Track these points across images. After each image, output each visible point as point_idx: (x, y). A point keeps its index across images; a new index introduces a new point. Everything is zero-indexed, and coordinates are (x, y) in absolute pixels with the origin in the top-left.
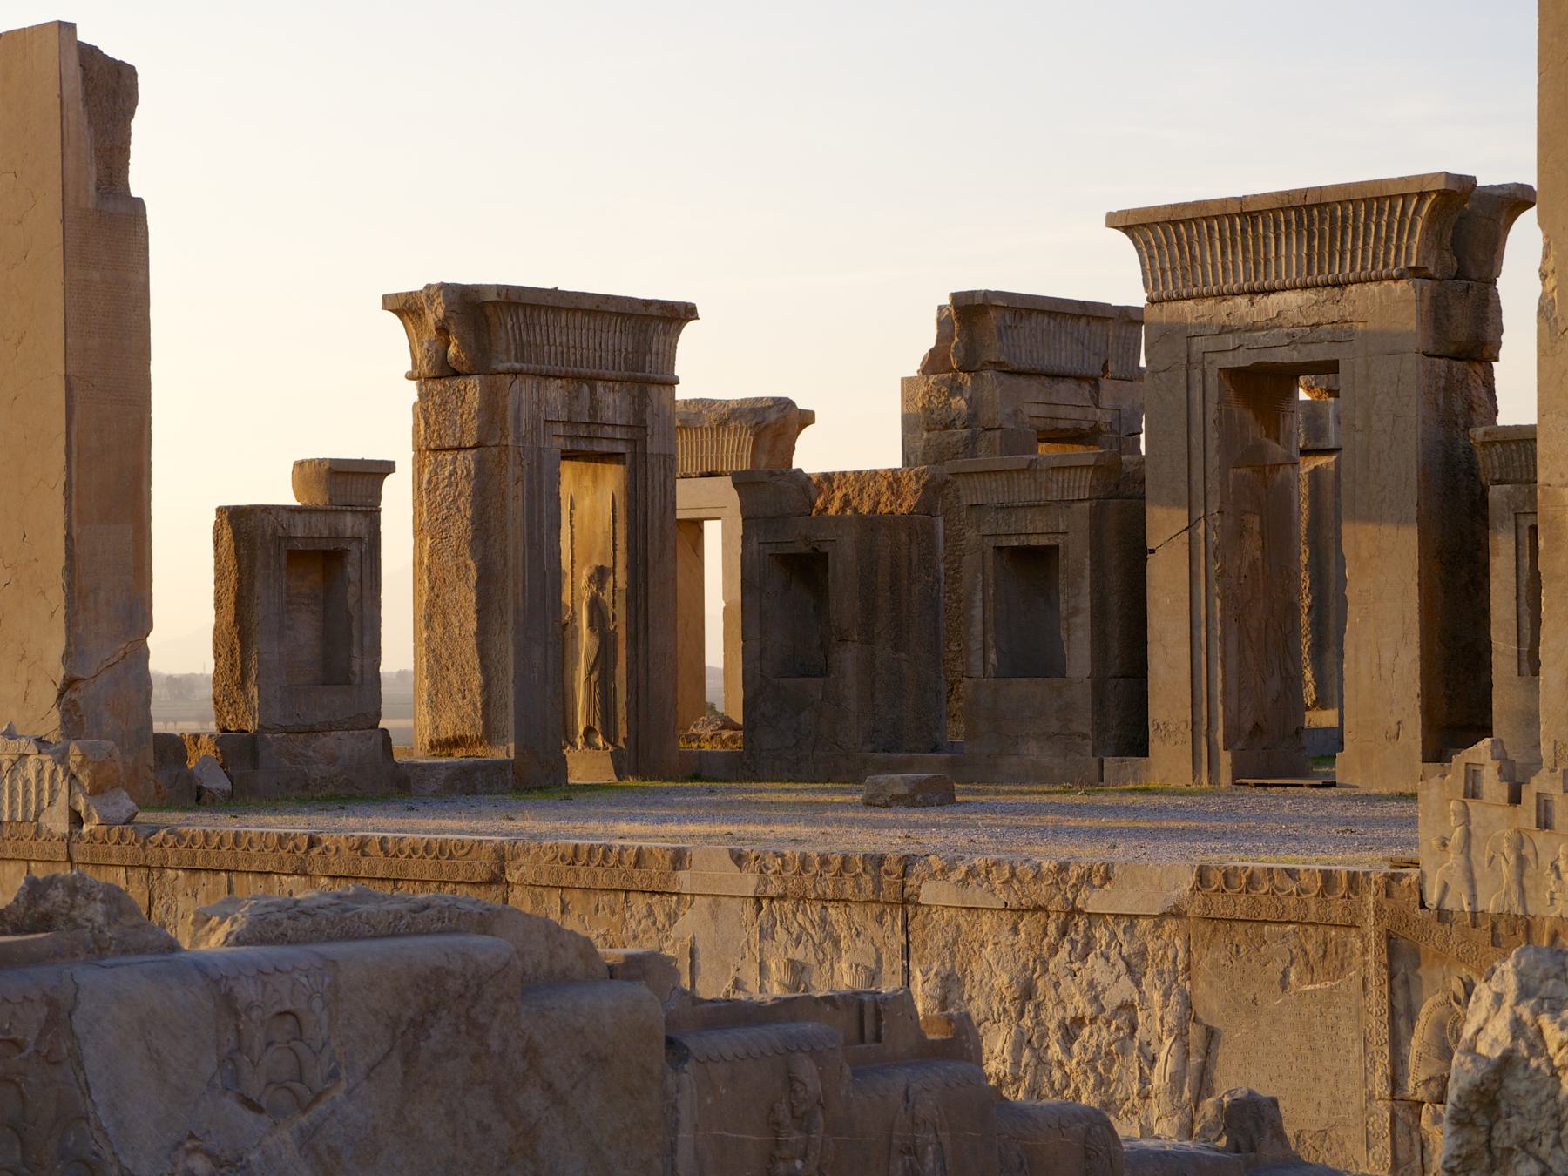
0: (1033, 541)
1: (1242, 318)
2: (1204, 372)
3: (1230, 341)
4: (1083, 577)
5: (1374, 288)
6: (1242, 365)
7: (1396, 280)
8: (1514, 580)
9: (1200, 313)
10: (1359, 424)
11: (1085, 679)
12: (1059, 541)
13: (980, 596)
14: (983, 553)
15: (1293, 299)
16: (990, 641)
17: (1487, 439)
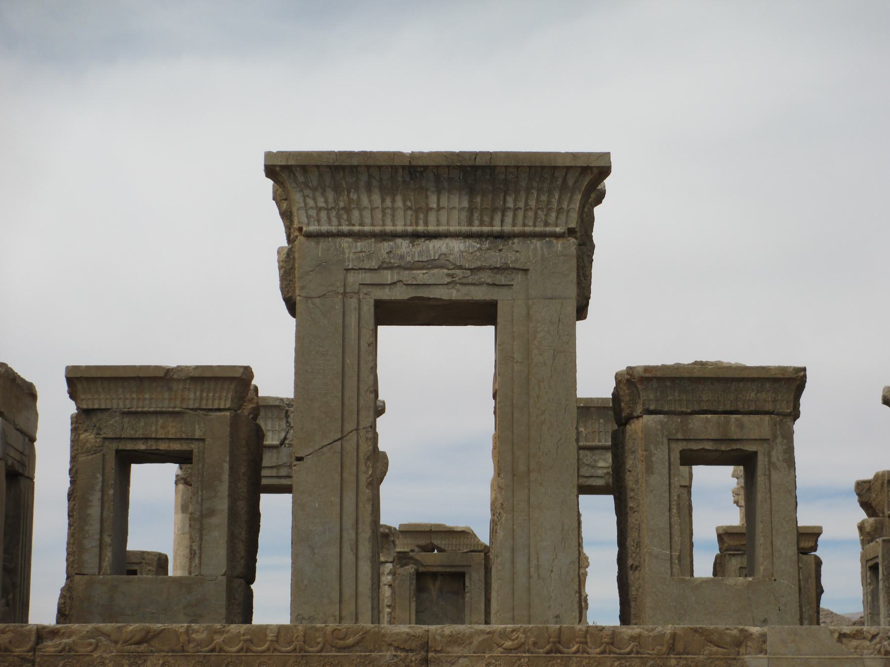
0: (163, 446)
1: (402, 257)
2: (359, 300)
3: (388, 276)
4: (221, 481)
5: (537, 243)
6: (399, 298)
7: (557, 236)
8: (667, 495)
9: (359, 249)
10: (517, 356)
11: (220, 578)
12: (194, 446)
13: (98, 495)
14: (104, 455)
15: (457, 246)
16: (107, 540)
17: (647, 375)
